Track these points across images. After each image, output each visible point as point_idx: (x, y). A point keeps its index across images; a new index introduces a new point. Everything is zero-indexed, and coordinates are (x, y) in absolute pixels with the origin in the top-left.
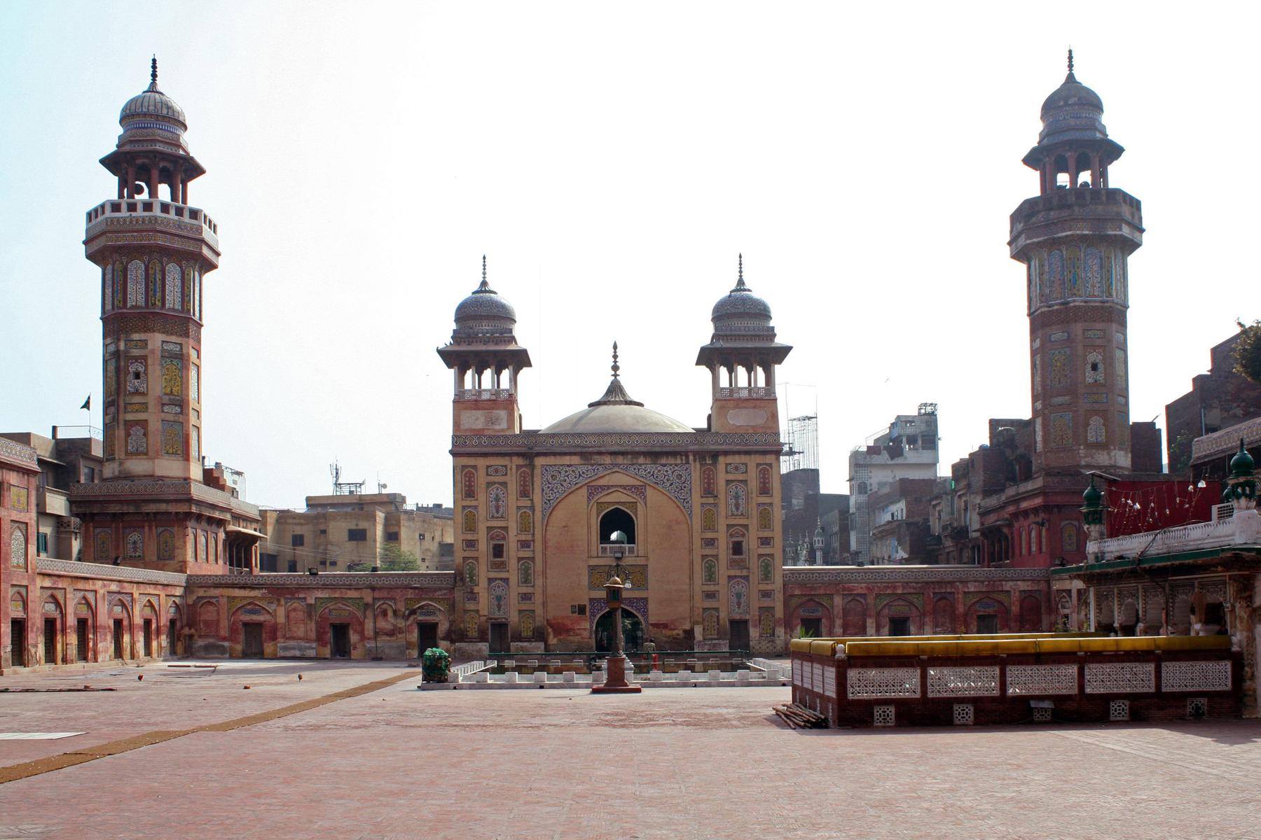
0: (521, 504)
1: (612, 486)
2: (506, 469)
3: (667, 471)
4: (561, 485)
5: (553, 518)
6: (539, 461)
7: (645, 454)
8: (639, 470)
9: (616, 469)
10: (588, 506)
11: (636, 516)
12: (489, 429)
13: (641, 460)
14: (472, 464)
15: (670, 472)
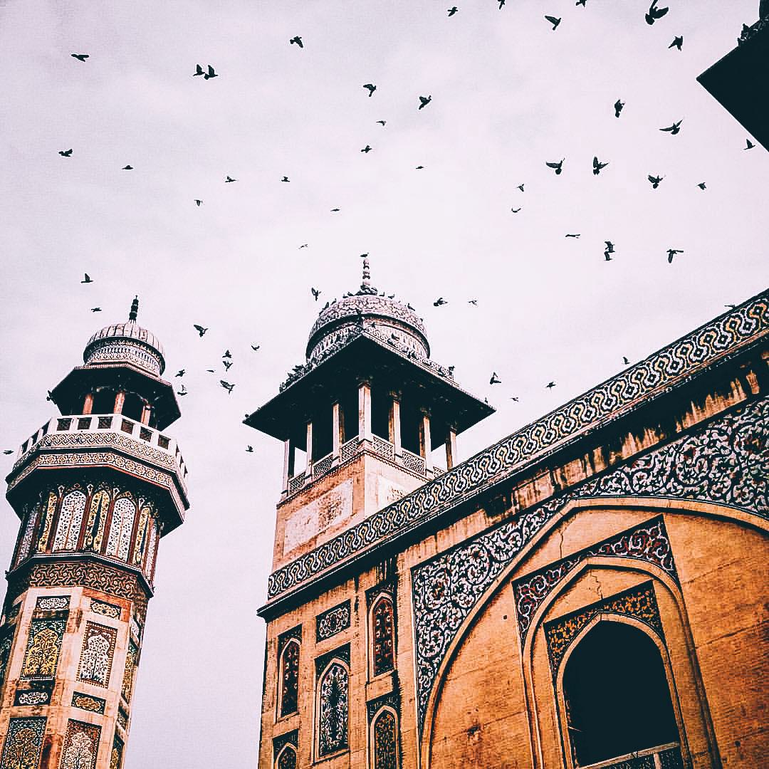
0: (374, 693)
1: (574, 557)
2: (349, 612)
3: (712, 444)
4: (455, 605)
5: (442, 715)
6: (409, 560)
7: (635, 422)
8: (630, 477)
9: (573, 504)
10: (523, 642)
11: (662, 636)
12: (324, 532)
13: (630, 447)
14: (293, 624)
15: (723, 442)
